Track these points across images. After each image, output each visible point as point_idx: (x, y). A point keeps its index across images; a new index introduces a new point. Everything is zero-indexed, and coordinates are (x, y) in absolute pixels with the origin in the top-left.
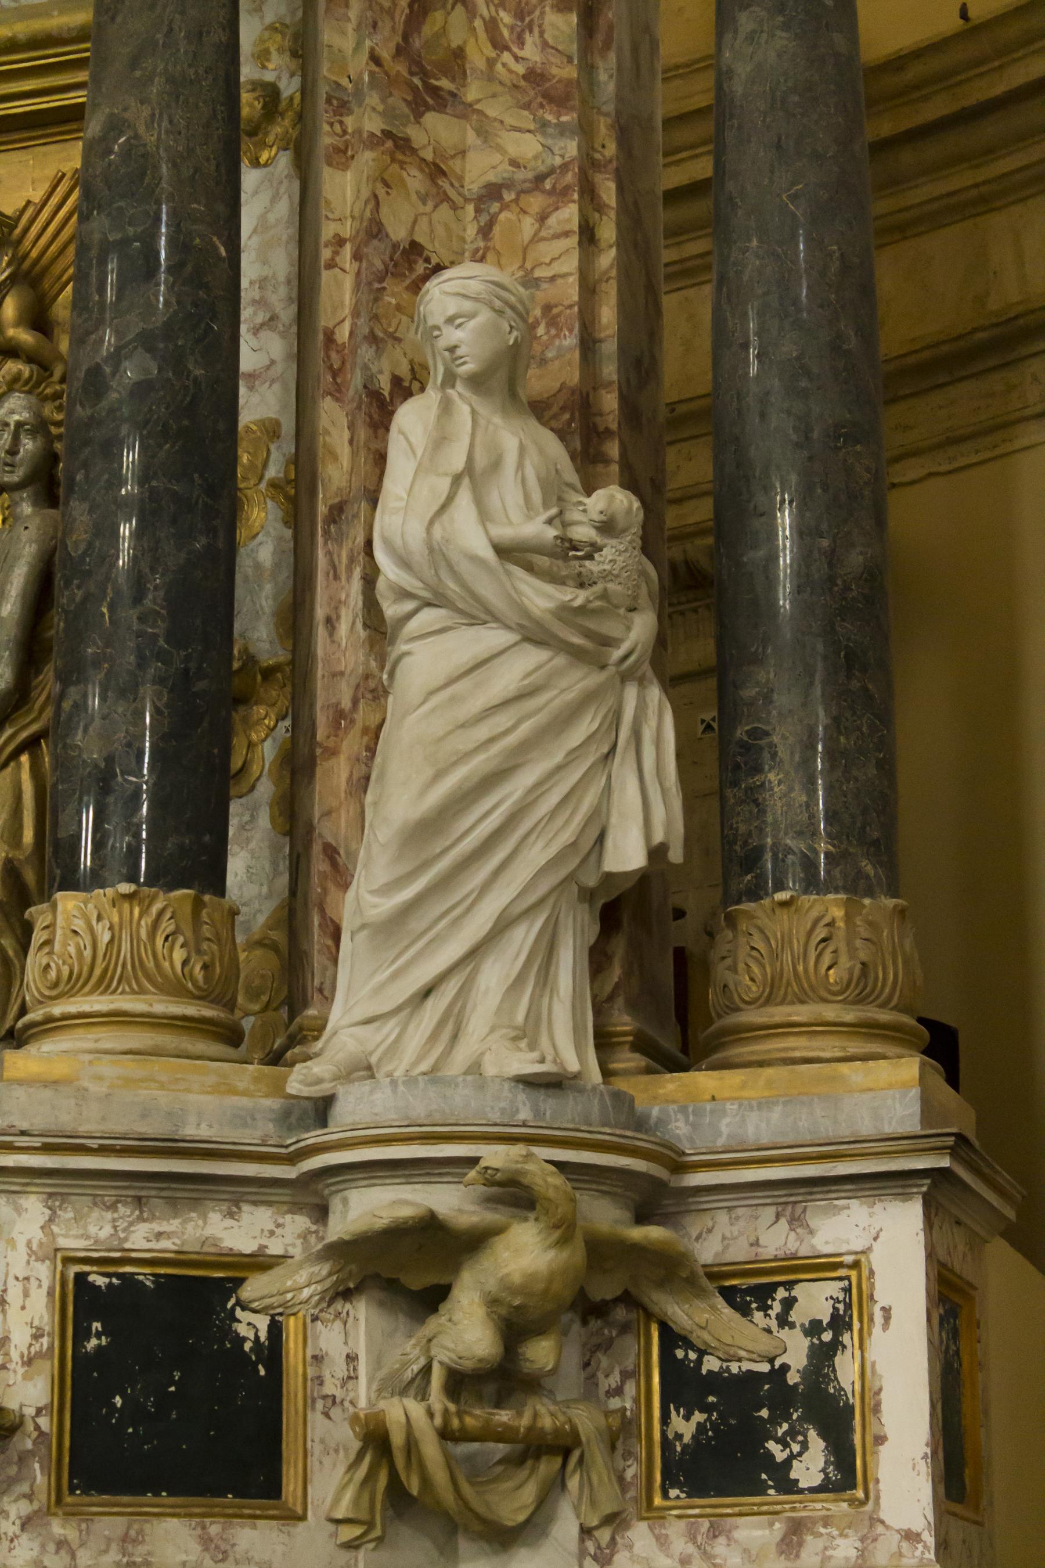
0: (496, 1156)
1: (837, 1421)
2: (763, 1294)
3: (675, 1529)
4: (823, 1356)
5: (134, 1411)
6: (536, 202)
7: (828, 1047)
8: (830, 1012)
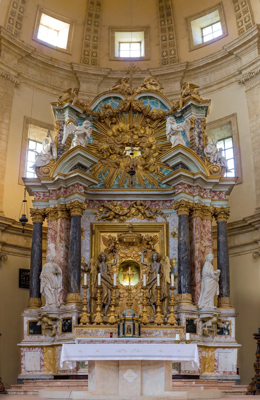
0: (215, 313)
1: (228, 331)
2: (224, 323)
3: (218, 337)
4: (228, 327)
5: (189, 328)
6: (209, 248)
7: (229, 307)
8: (228, 305)
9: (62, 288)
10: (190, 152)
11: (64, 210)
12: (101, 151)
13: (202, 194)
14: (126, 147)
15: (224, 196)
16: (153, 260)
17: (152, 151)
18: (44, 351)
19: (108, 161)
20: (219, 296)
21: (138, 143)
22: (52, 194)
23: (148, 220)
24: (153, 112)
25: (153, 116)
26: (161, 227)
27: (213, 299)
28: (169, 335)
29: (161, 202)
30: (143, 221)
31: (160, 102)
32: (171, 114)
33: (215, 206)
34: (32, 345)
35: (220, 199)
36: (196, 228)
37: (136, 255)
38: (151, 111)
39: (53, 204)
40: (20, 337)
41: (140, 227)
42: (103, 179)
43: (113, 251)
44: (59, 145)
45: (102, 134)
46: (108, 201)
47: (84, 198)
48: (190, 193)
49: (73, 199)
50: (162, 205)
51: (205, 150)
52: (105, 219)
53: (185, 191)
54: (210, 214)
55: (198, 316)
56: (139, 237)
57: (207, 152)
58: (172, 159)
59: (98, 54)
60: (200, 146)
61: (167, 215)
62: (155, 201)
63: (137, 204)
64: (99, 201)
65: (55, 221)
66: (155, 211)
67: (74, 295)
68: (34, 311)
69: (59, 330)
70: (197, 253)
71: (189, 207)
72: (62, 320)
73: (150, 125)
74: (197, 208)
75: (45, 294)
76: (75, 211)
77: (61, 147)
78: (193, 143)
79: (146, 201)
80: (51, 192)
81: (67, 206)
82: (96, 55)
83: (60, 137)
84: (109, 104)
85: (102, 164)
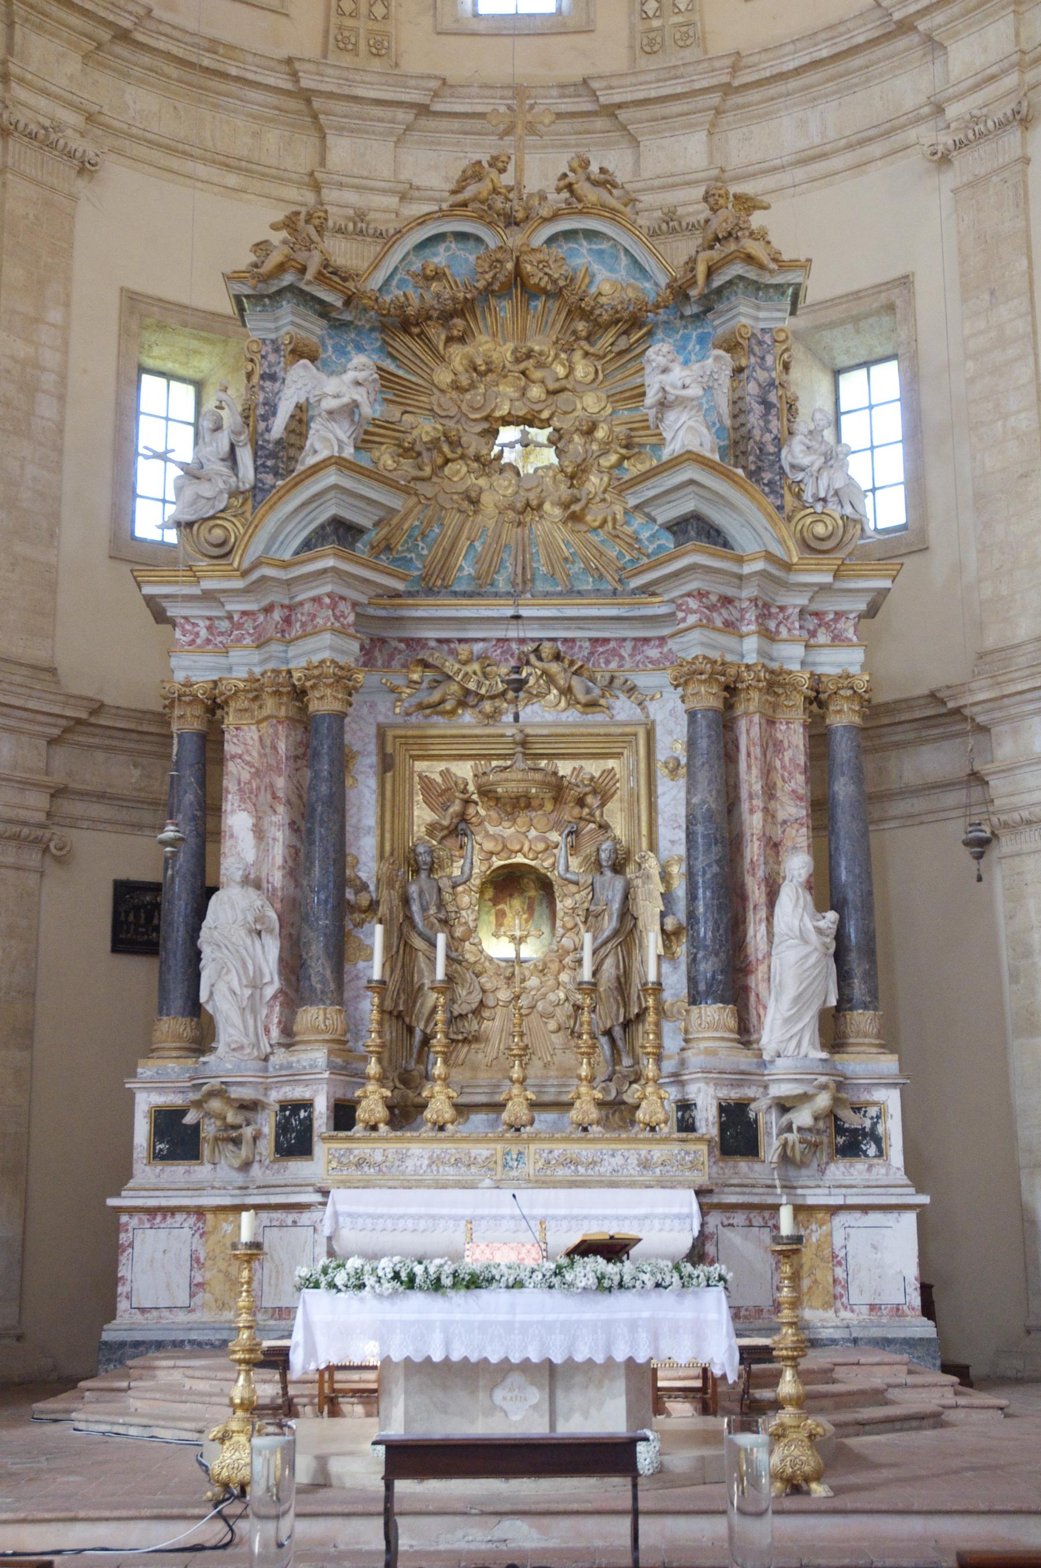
0: (823, 1079)
1: (878, 1141)
5: (731, 1136)
6: (796, 826)
7: (874, 1050)
9: (277, 985)
10: (729, 476)
11: (284, 690)
12: (412, 449)
13: (772, 625)
14: (501, 429)
15: (851, 630)
16: (601, 866)
17: (595, 447)
18: (208, 1228)
19: (437, 488)
20: (838, 1008)
21: (545, 415)
22: (239, 626)
23: (583, 713)
24: (600, 294)
25: (597, 312)
26: (627, 739)
27: (815, 1025)
28: (658, 1170)
29: (629, 645)
30: (564, 717)
31: (626, 251)
32: (666, 307)
33: (819, 670)
34: (164, 1202)
35: (837, 643)
36: (749, 755)
37: (541, 846)
38: (593, 290)
39: (243, 664)
40: (121, 1174)
41: (552, 740)
42: (420, 556)
43: (459, 829)
44: (262, 434)
45: (414, 379)
46: (440, 641)
47: (355, 646)
48: (730, 627)
49: (314, 651)
50: (632, 656)
51: (784, 452)
52: (428, 711)
53: (708, 619)
54: (800, 700)
55: (761, 1090)
56: (549, 784)
57: (795, 462)
58: (665, 499)
59: (393, 10)
60: (768, 437)
61: (650, 692)
62: (606, 641)
63: (544, 655)
64: (408, 642)
65: (253, 727)
66: (608, 678)
67: (321, 1013)
68: (175, 1068)
69: (267, 1146)
70: (753, 850)
71: (723, 679)
72: (277, 1107)
73: (587, 347)
74: (754, 683)
75: (214, 1007)
76: (322, 698)
77: (268, 442)
78: (743, 425)
79: (573, 640)
80: (236, 618)
81: (296, 675)
82: (385, 11)
83: (265, 404)
84: (436, 260)
85: (414, 499)
